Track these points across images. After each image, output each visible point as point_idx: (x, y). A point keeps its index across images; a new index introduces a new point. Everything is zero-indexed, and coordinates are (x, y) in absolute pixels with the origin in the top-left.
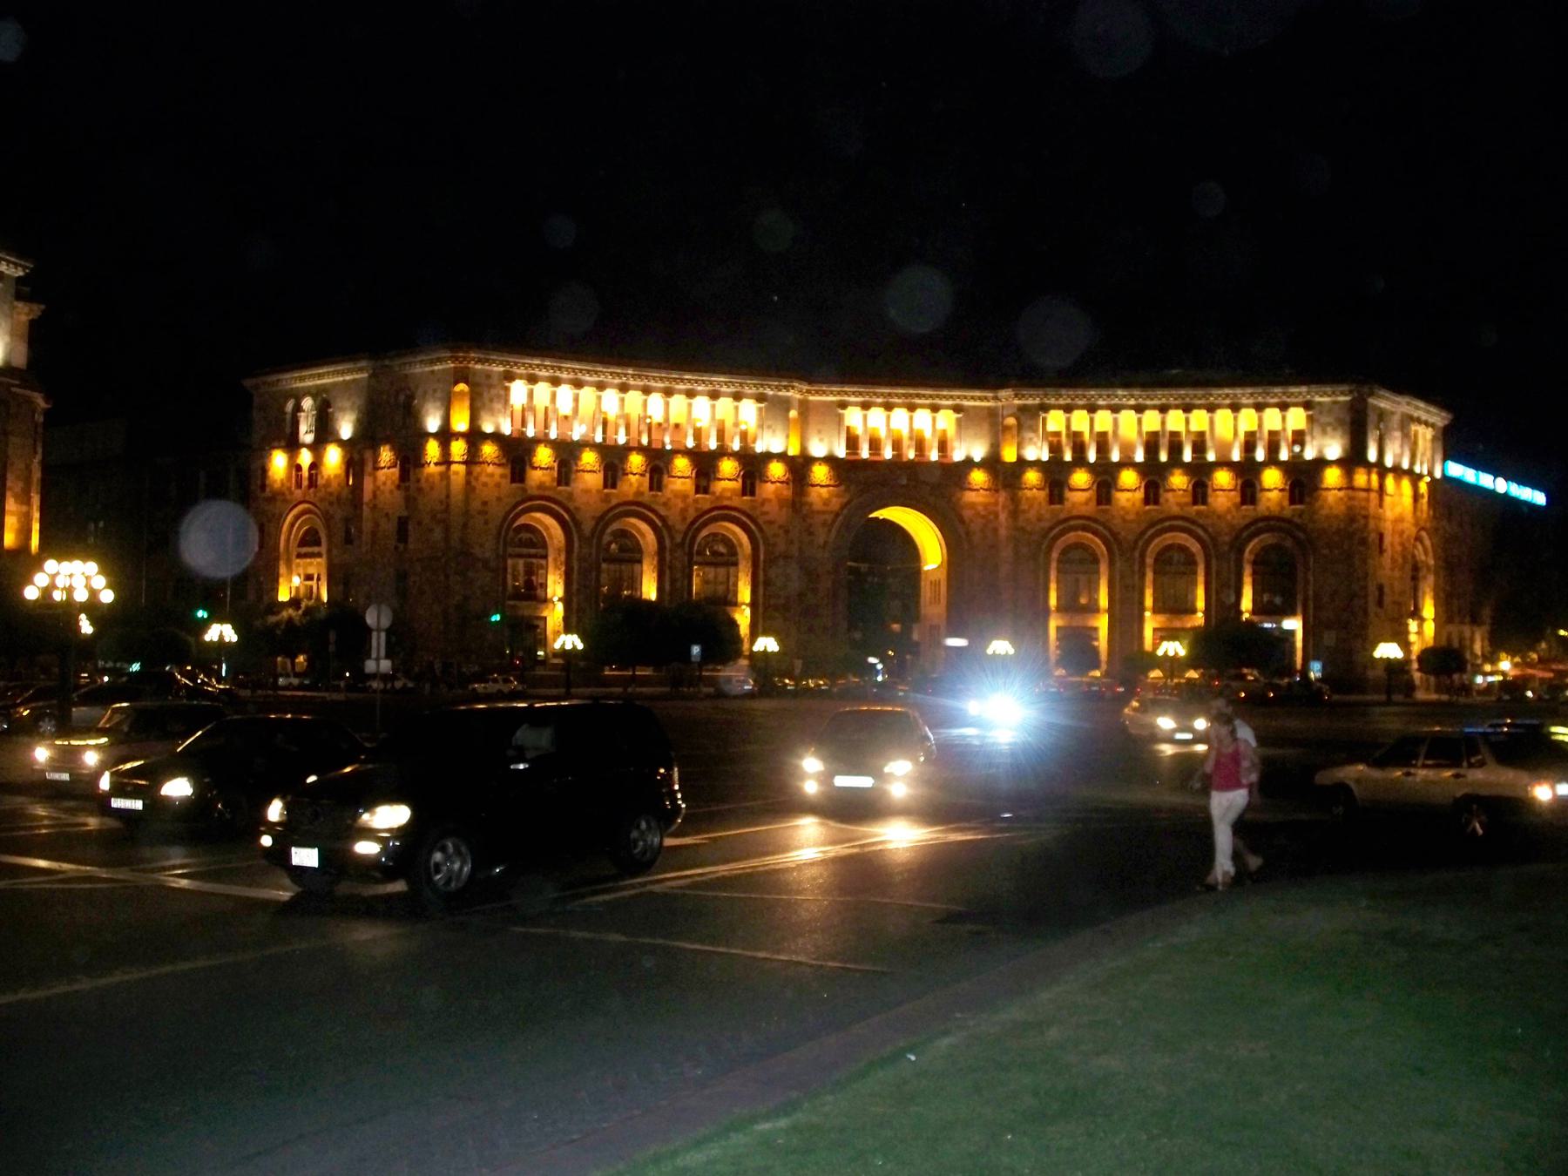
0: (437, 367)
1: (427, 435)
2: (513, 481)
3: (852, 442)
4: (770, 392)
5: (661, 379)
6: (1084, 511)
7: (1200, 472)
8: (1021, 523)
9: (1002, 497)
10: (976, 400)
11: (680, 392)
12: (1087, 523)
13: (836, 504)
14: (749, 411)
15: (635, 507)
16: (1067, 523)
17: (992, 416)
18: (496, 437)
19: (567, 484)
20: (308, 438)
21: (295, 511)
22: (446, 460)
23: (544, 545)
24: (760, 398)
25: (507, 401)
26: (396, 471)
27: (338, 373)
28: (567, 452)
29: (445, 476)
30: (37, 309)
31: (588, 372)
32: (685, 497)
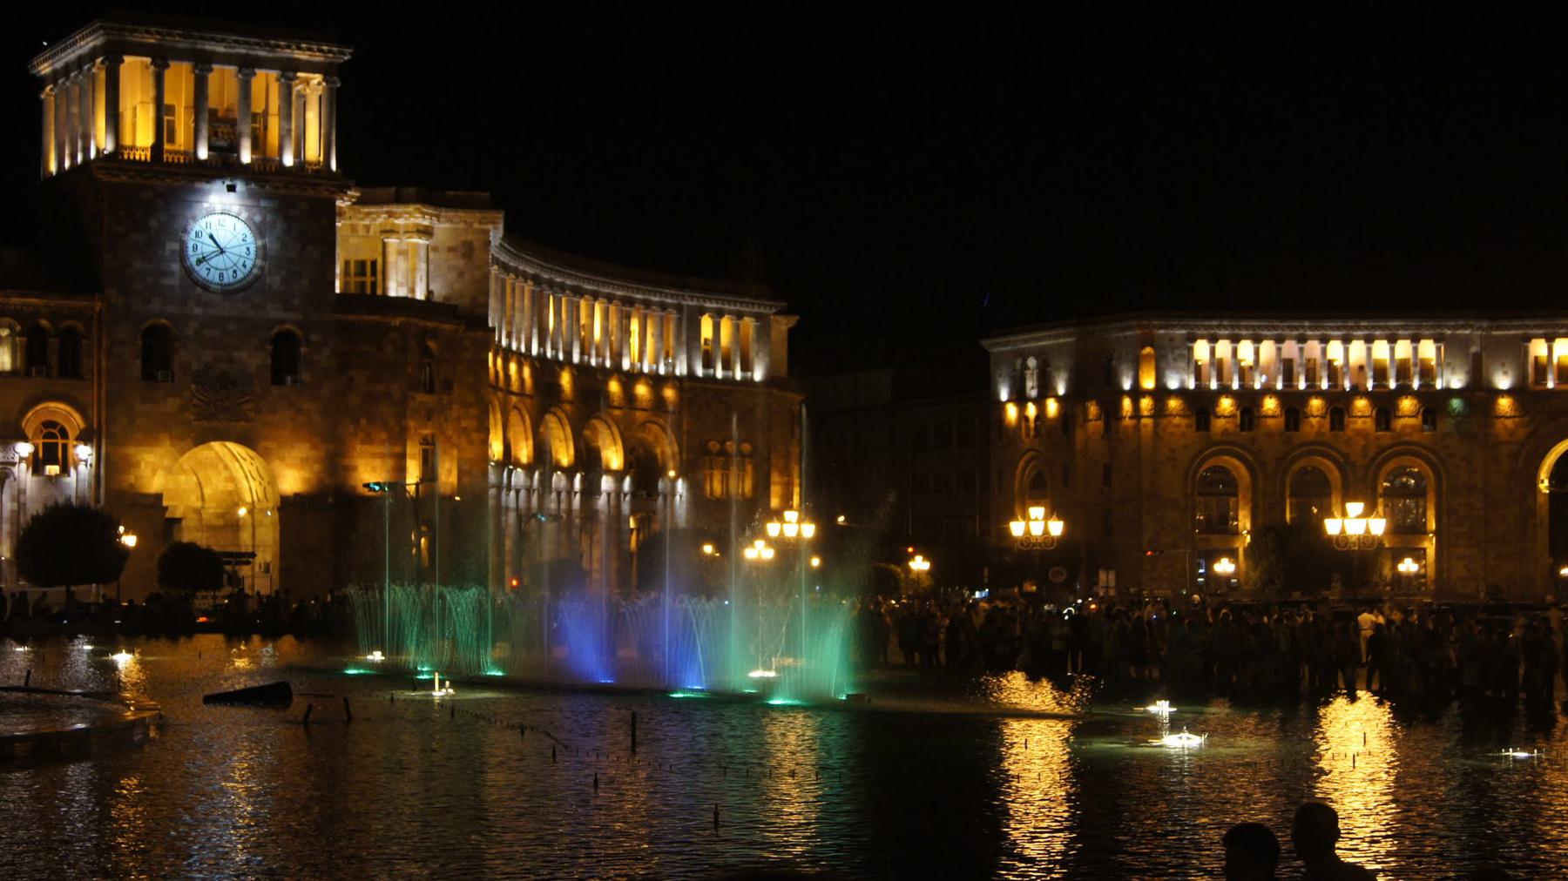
0: (1128, 333)
2: (1198, 429)
5: (1338, 328)
11: (1358, 338)
13: (1521, 434)
14: (1428, 349)
18: (1182, 392)
19: (1250, 429)
20: (1033, 393)
21: (1026, 457)
23: (1236, 486)
24: (1437, 340)
26: (1100, 423)
27: (1049, 337)
28: (1248, 400)
29: (1137, 428)
30: (793, 320)
31: (1267, 328)
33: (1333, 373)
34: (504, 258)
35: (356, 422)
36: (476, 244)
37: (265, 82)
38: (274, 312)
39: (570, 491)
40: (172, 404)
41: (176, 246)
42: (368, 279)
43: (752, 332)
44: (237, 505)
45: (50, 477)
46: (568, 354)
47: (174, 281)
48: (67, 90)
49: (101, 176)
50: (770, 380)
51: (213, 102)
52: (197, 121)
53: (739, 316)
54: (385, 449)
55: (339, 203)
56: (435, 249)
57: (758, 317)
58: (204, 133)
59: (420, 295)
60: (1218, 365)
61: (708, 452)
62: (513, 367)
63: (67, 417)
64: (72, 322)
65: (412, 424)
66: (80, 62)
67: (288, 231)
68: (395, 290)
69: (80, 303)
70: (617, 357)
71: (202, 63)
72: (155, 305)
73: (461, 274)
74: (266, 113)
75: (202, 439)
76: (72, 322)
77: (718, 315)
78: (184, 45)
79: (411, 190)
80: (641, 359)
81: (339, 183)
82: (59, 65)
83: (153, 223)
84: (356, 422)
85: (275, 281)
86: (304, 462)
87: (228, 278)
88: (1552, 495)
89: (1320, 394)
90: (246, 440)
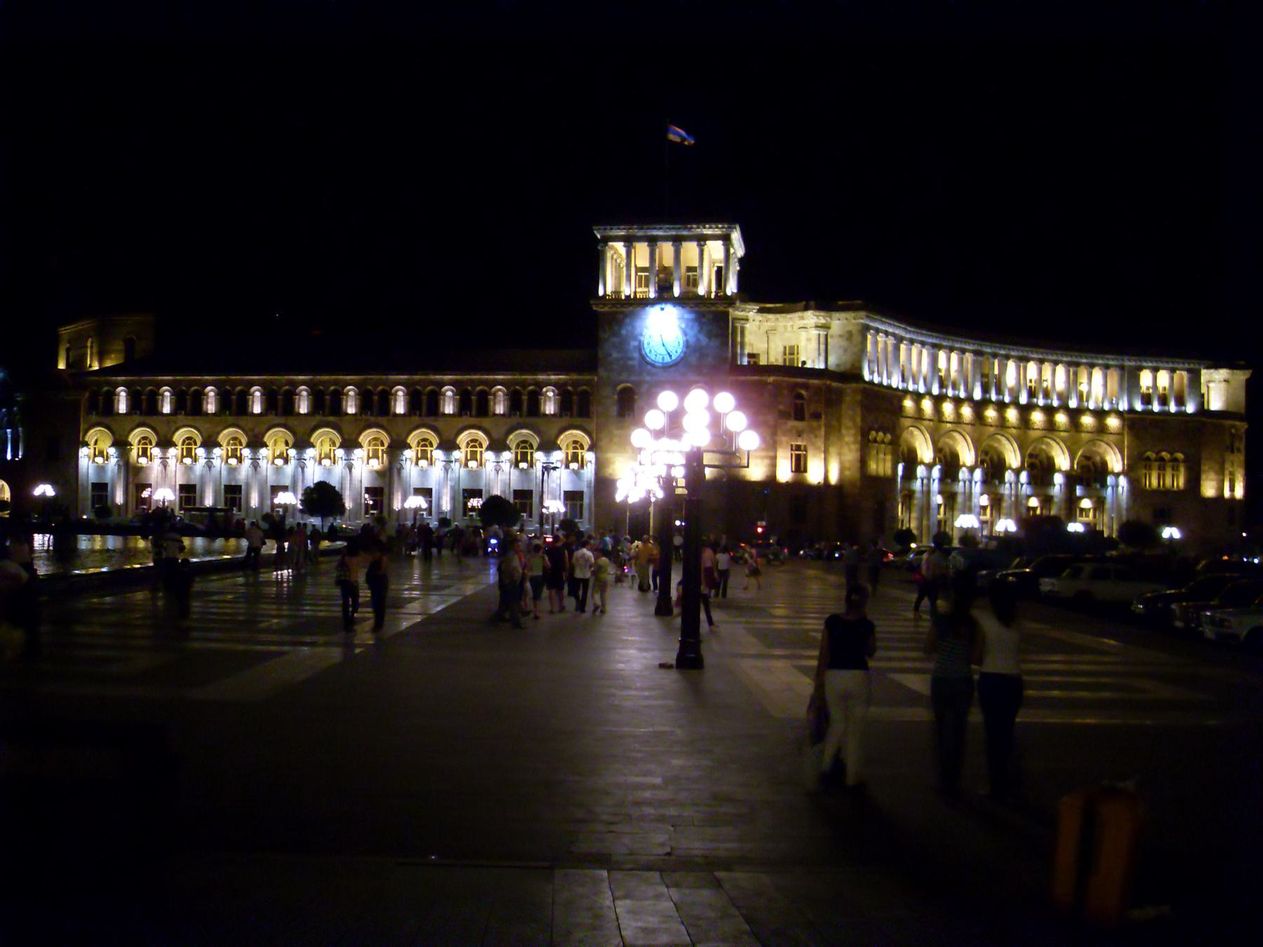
34: (930, 340)
37: (690, 248)
41: (636, 343)
43: (1186, 381)
47: (635, 363)
55: (734, 313)
57: (1189, 371)
61: (1148, 459)
62: (948, 408)
69: (587, 377)
72: (624, 376)
73: (845, 351)
78: (641, 233)
79: (812, 303)
81: (730, 301)
83: (624, 332)
87: (667, 359)
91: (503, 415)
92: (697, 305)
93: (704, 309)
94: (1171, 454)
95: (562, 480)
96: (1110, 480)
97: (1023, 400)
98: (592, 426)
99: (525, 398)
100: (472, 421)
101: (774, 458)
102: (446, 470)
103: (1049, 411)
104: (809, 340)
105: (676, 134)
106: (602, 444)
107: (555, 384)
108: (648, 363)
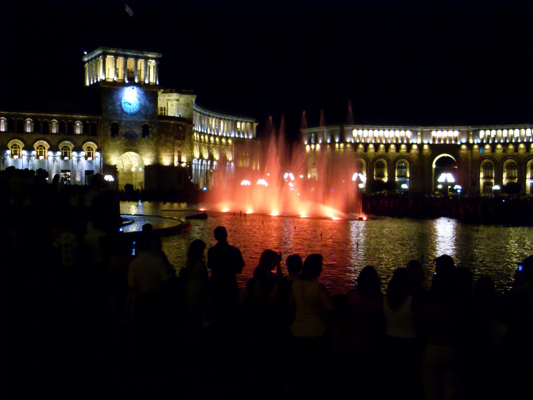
1: (336, 143)
3: (434, 140)
4: (413, 129)
6: (488, 154)
7: (516, 144)
8: (473, 157)
9: (469, 151)
10: (464, 129)
12: (489, 157)
13: (430, 154)
14: (409, 134)
15: (382, 156)
16: (483, 158)
17: (468, 132)
18: (350, 143)
20: (313, 142)
22: (339, 148)
24: (411, 131)
25: (352, 135)
28: (366, 145)
29: (339, 151)
32: (393, 153)
33: (386, 139)
34: (194, 107)
35: (162, 147)
36: (190, 103)
37: (141, 62)
38: (143, 120)
39: (207, 165)
40: (119, 142)
41: (119, 103)
42: (163, 112)
44: (131, 168)
45: (89, 161)
46: (207, 131)
47: (119, 112)
48: (92, 65)
49: (101, 85)
50: (253, 138)
51: (128, 68)
52: (124, 72)
53: (246, 122)
54: (169, 154)
55: (159, 93)
56: (180, 104)
57: (251, 123)
58: (126, 75)
59: (177, 116)
60: (358, 136)
63: (93, 146)
64: (94, 122)
65: (176, 148)
66: (95, 58)
67: (146, 99)
68: (170, 114)
70: (218, 132)
71: (126, 57)
72: (114, 118)
73: (186, 111)
74: (140, 70)
75: (125, 152)
76: (94, 122)
77: (241, 122)
78: (121, 53)
79: (174, 90)
80: (223, 133)
82: (90, 58)
83: (114, 97)
84: (162, 147)
85: (143, 112)
86: (150, 157)
87: (132, 111)
88: (435, 169)
89: (383, 144)
90: (136, 151)
91: (56, 134)
92: (146, 88)
93: (149, 90)
94: (246, 154)
95: (84, 165)
96: (228, 163)
97: (209, 133)
98: (99, 140)
99: (66, 126)
100: (41, 136)
101: (173, 156)
102: (28, 161)
103: (215, 136)
104: (172, 105)
105: (128, 10)
106: (105, 149)
107: (81, 120)
108: (124, 112)
